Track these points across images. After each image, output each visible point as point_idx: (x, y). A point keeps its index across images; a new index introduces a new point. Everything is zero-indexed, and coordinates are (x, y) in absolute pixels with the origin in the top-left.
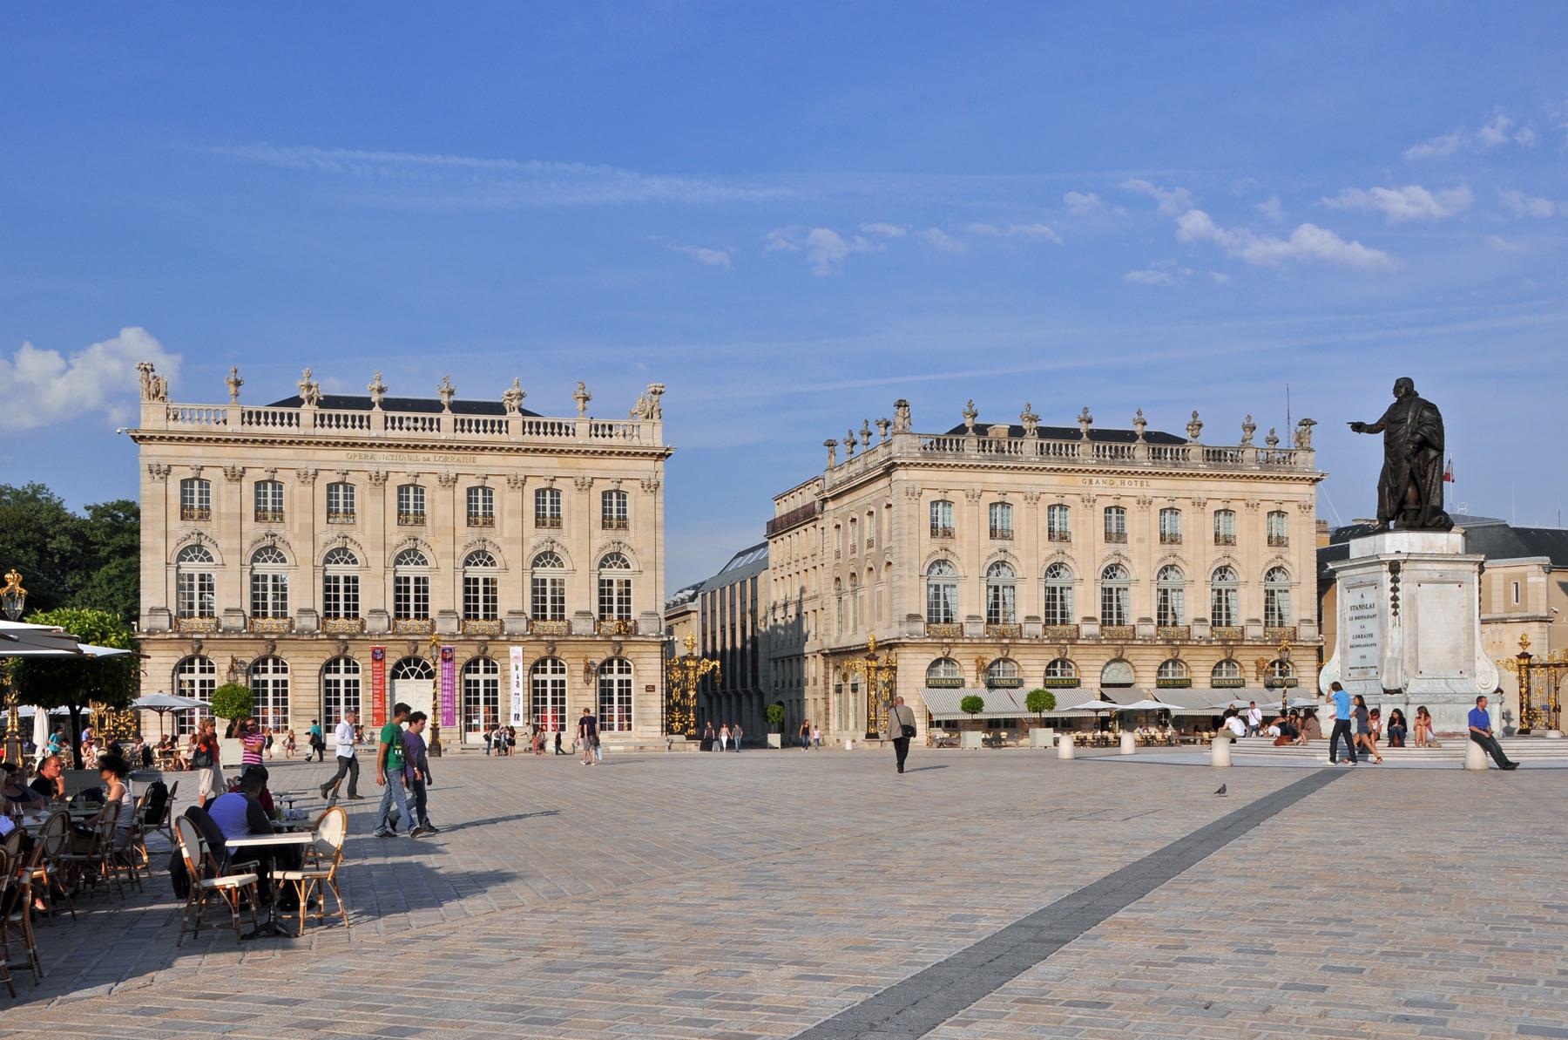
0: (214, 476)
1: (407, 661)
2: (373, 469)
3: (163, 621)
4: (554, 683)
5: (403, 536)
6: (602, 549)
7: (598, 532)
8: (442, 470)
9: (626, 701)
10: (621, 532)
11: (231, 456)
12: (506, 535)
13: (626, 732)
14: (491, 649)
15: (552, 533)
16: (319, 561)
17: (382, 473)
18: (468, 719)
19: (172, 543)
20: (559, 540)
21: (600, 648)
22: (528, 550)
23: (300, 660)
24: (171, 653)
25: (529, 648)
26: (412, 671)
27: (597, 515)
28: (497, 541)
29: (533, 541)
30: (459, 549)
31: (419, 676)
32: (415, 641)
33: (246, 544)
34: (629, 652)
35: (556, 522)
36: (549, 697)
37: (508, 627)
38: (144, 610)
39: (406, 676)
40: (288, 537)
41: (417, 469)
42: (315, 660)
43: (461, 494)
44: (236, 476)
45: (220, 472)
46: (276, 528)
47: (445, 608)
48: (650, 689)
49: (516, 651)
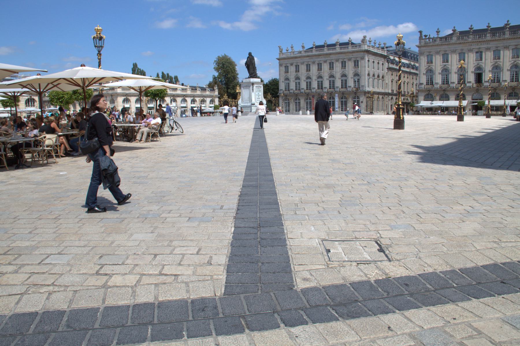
2: (312, 60)
3: (282, 92)
7: (353, 69)
8: (324, 59)
11: (291, 61)
48: (362, 102)
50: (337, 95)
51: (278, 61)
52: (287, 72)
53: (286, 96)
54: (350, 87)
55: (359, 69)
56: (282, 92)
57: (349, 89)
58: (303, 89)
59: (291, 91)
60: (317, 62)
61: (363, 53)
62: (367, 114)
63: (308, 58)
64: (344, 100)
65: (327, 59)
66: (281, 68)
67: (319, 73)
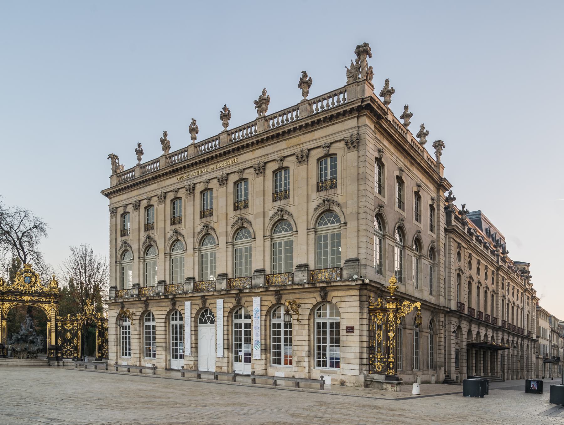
13: (335, 369)
18: (236, 353)
21: (312, 295)
22: (267, 220)
24: (114, 311)
25: (265, 298)
26: (209, 318)
27: (314, 181)
29: (271, 213)
32: (203, 297)
33: (141, 244)
34: (334, 296)
37: (253, 282)
39: (205, 322)
41: (205, 177)
47: (221, 272)
48: (350, 330)
49: (257, 301)
50: (257, 301)
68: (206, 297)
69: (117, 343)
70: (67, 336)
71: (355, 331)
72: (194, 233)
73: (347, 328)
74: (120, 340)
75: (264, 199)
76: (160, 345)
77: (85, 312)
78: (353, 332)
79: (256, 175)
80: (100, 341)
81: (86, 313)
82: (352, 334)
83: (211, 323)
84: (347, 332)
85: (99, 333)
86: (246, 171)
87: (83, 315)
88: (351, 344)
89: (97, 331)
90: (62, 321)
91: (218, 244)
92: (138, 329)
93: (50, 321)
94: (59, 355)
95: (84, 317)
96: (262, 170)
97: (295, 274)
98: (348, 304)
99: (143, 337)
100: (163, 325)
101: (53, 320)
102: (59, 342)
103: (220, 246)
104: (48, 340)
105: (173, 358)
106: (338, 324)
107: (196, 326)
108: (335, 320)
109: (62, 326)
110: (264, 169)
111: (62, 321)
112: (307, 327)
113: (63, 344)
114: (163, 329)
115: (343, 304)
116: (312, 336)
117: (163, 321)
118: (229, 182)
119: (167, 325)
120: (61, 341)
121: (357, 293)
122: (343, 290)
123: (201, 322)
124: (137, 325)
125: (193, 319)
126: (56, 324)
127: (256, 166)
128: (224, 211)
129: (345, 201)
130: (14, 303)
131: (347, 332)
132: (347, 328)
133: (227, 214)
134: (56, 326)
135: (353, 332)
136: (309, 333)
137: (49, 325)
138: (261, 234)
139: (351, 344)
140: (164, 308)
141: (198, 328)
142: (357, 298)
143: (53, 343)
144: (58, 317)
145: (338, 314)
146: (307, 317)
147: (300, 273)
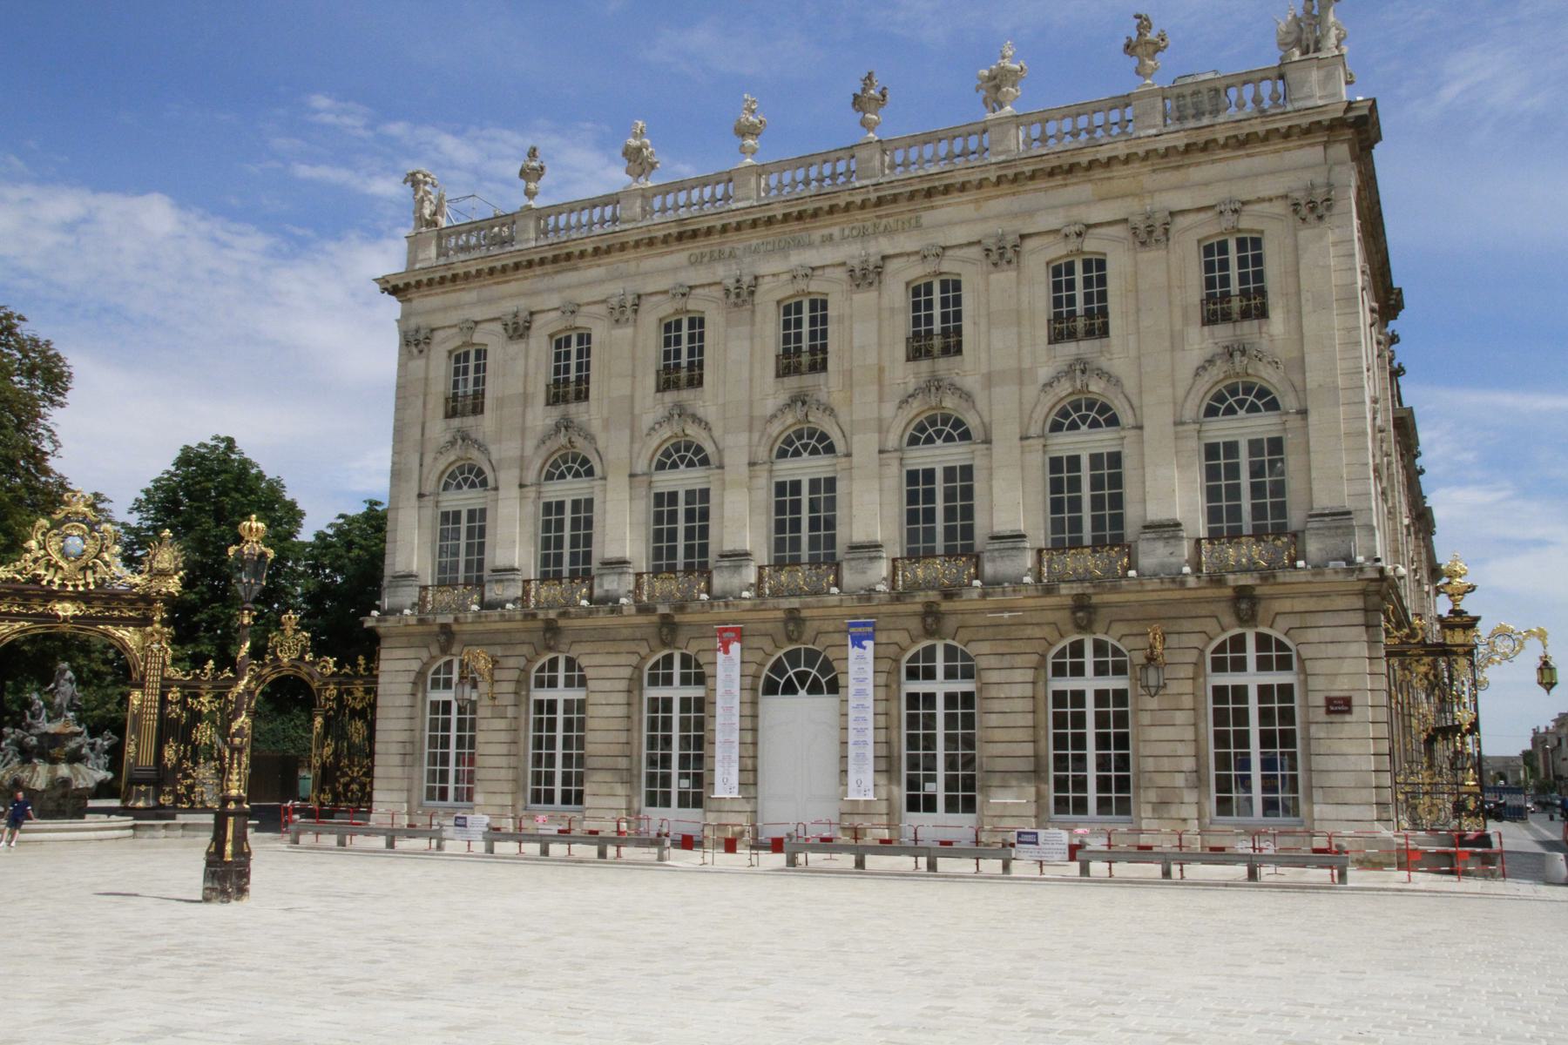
0: (491, 337)
1: (793, 657)
2: (723, 272)
3: (408, 595)
4: (1101, 697)
5: (783, 398)
6: (1200, 370)
8: (852, 252)
9: (1280, 738)
10: (1248, 328)
12: (984, 369)
14: (950, 623)
15: (1086, 348)
16: (641, 466)
17: (747, 280)
19: (428, 459)
20: (1104, 363)
22: (1031, 391)
23: (598, 660)
24: (411, 653)
26: (802, 677)
28: (971, 382)
29: (1044, 373)
30: (889, 409)
31: (815, 689)
35: (1098, 327)
36: (1091, 731)
37: (989, 569)
38: (385, 582)
39: (790, 689)
40: (596, 426)
42: (623, 659)
43: (895, 294)
44: (518, 329)
45: (498, 327)
46: (575, 410)
48: (1339, 706)
51: (392, 308)
52: (465, 403)
53: (447, 637)
54: (1168, 530)
55: (1277, 322)
56: (408, 595)
57: (1153, 555)
58: (618, 565)
59: (493, 592)
60: (771, 294)
61: (1310, 154)
62: (1408, 860)
63: (679, 256)
64: (1089, 684)
65: (885, 245)
66: (418, 365)
67: (799, 399)
68: (805, 613)
69: (408, 756)
70: (196, 734)
71: (1355, 710)
72: (752, 418)
73: (1330, 701)
74: (422, 749)
75: (1019, 335)
76: (610, 762)
77: (274, 653)
78: (1349, 712)
79: (992, 268)
80: (328, 751)
81: (277, 659)
82: (1348, 718)
83: (810, 692)
84: (1329, 712)
85: (327, 725)
86: (949, 253)
87: (264, 666)
88: (1345, 747)
89: (319, 721)
90: (183, 686)
91: (848, 455)
92: (510, 712)
93: (141, 685)
94: (167, 800)
95: (266, 671)
96: (1009, 254)
97: (1142, 546)
98: (1328, 634)
99: (526, 737)
100: (622, 698)
101: (153, 680)
102: (169, 754)
103: (855, 459)
104: (131, 749)
105: (651, 801)
106: (1286, 691)
107: (754, 703)
108: (1275, 678)
109: (183, 702)
110: (1017, 253)
111: (183, 686)
112: (1188, 702)
113: (180, 761)
114: (621, 711)
115: (1312, 635)
116: (1202, 725)
117: (623, 685)
118: (887, 279)
119: (635, 700)
120: (177, 752)
121: (1359, 603)
122: (1311, 595)
123: (771, 689)
124: (510, 699)
125: (748, 680)
126: (163, 697)
127: (990, 243)
128: (872, 359)
129: (1295, 354)
130: (17, 626)
131: (1329, 712)
132: (1330, 701)
133: (881, 370)
134: (164, 701)
135: (1349, 712)
136: (1197, 717)
137: (136, 697)
138: (1014, 430)
139: (1345, 747)
140: (625, 646)
141: (760, 707)
142: (1359, 618)
143: (147, 759)
144: (171, 672)
145: (1285, 664)
146: (1188, 671)
147: (1160, 545)
